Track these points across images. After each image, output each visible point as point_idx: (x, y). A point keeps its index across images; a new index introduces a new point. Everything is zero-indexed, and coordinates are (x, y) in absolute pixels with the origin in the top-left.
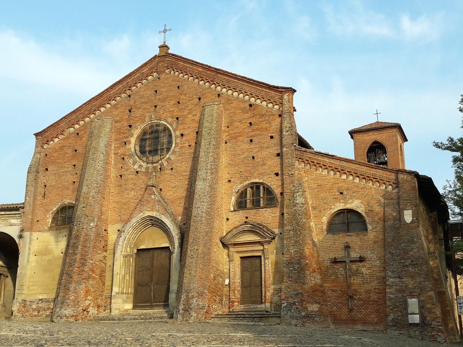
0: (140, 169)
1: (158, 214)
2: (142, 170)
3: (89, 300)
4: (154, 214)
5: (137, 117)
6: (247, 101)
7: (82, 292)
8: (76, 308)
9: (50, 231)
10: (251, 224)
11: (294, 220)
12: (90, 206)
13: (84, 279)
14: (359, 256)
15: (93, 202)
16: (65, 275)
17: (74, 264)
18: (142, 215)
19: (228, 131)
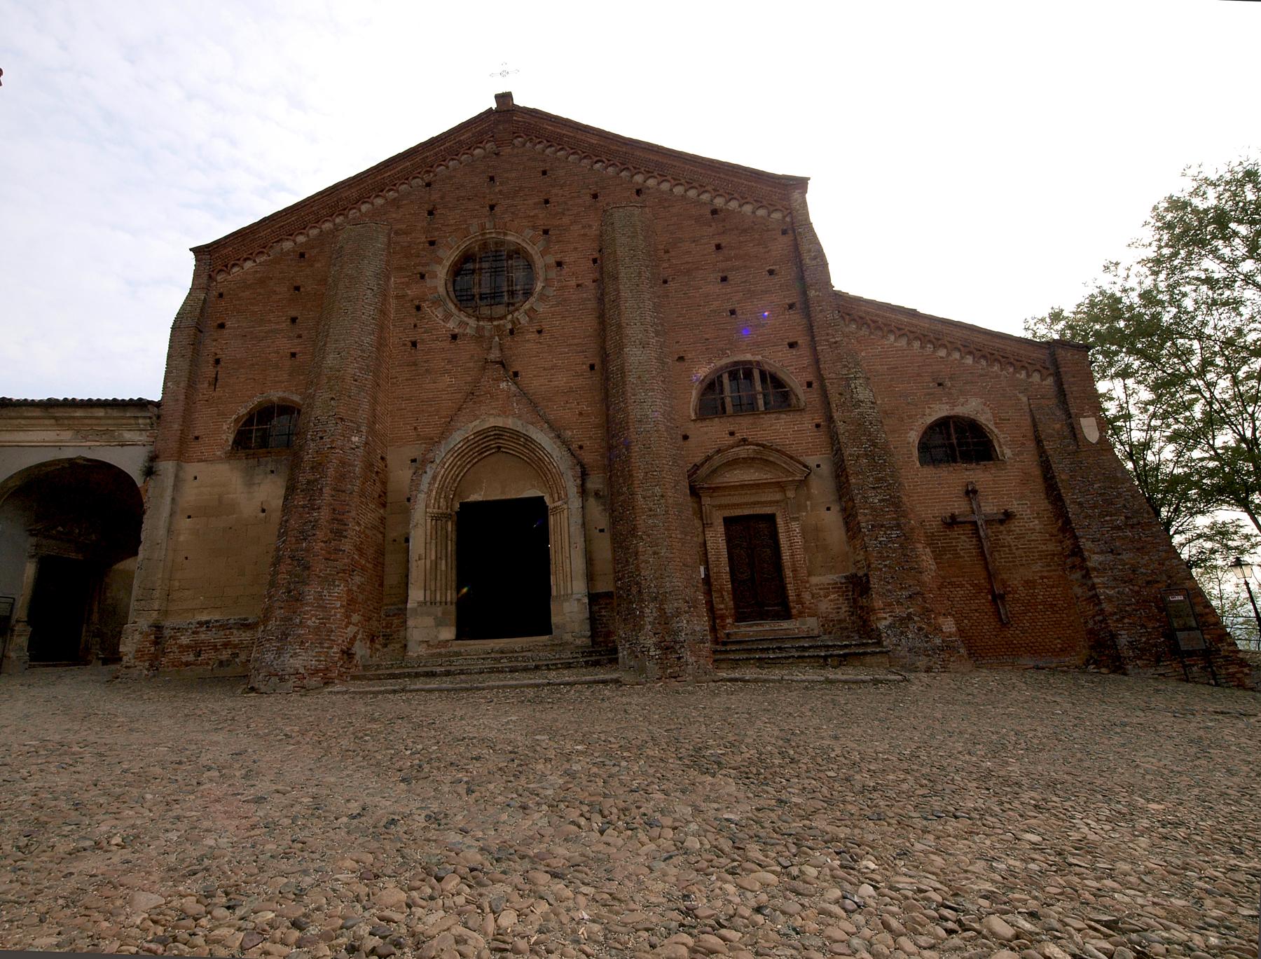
0: (461, 331)
1: (519, 423)
2: (468, 331)
3: (353, 625)
4: (510, 423)
5: (448, 225)
6: (705, 203)
7: (339, 606)
8: (323, 648)
9: (231, 462)
10: (757, 445)
11: (865, 435)
12: (350, 397)
13: (344, 571)
15: (354, 390)
16: (289, 561)
17: (314, 532)
18: (477, 425)
19: (669, 260)
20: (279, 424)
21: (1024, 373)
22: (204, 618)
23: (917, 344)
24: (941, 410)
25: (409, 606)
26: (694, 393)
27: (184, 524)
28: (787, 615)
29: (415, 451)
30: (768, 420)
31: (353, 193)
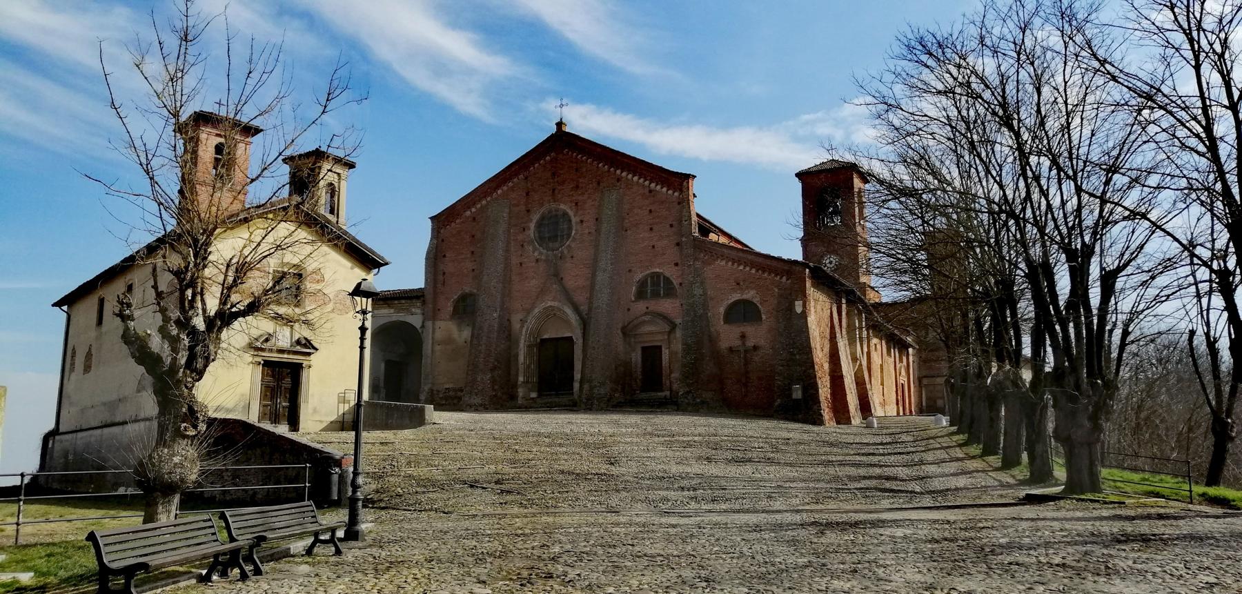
4: (556, 304)
14: (753, 344)
21: (779, 277)
22: (447, 387)
23: (730, 263)
24: (736, 297)
25: (519, 383)
26: (634, 288)
27: (438, 348)
28: (662, 391)
30: (662, 301)
31: (493, 185)
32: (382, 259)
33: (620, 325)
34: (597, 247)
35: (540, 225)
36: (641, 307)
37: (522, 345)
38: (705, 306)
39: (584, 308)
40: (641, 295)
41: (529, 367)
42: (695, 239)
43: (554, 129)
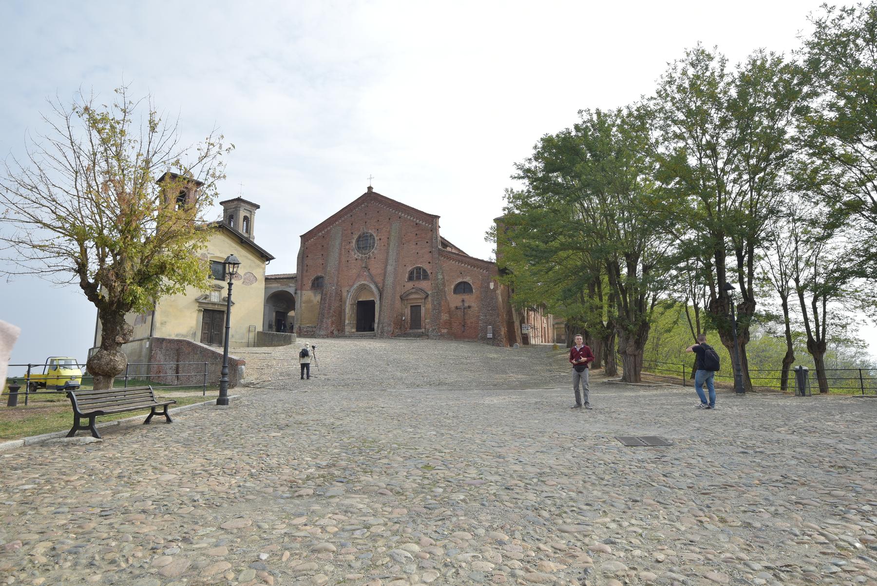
4: (366, 282)
18: (359, 283)
20: (320, 280)
24: (460, 280)
29: (347, 289)
30: (422, 282)
32: (271, 256)
33: (399, 294)
34: (388, 253)
35: (358, 241)
36: (410, 285)
37: (348, 303)
38: (444, 284)
39: (380, 285)
40: (411, 278)
41: (351, 315)
42: (439, 250)
43: (366, 191)
